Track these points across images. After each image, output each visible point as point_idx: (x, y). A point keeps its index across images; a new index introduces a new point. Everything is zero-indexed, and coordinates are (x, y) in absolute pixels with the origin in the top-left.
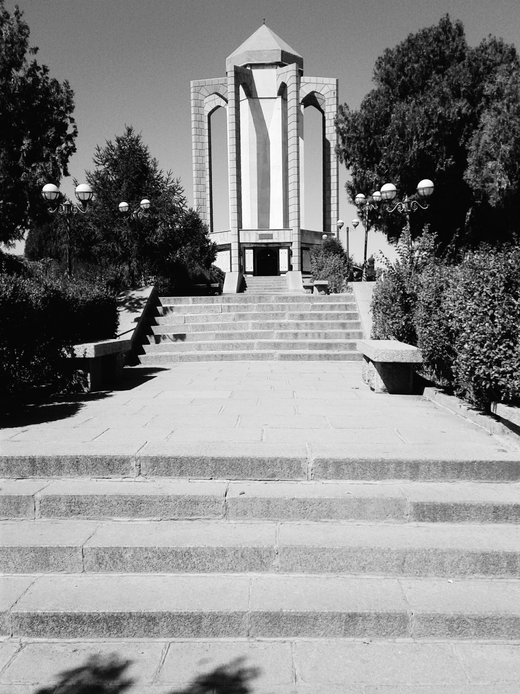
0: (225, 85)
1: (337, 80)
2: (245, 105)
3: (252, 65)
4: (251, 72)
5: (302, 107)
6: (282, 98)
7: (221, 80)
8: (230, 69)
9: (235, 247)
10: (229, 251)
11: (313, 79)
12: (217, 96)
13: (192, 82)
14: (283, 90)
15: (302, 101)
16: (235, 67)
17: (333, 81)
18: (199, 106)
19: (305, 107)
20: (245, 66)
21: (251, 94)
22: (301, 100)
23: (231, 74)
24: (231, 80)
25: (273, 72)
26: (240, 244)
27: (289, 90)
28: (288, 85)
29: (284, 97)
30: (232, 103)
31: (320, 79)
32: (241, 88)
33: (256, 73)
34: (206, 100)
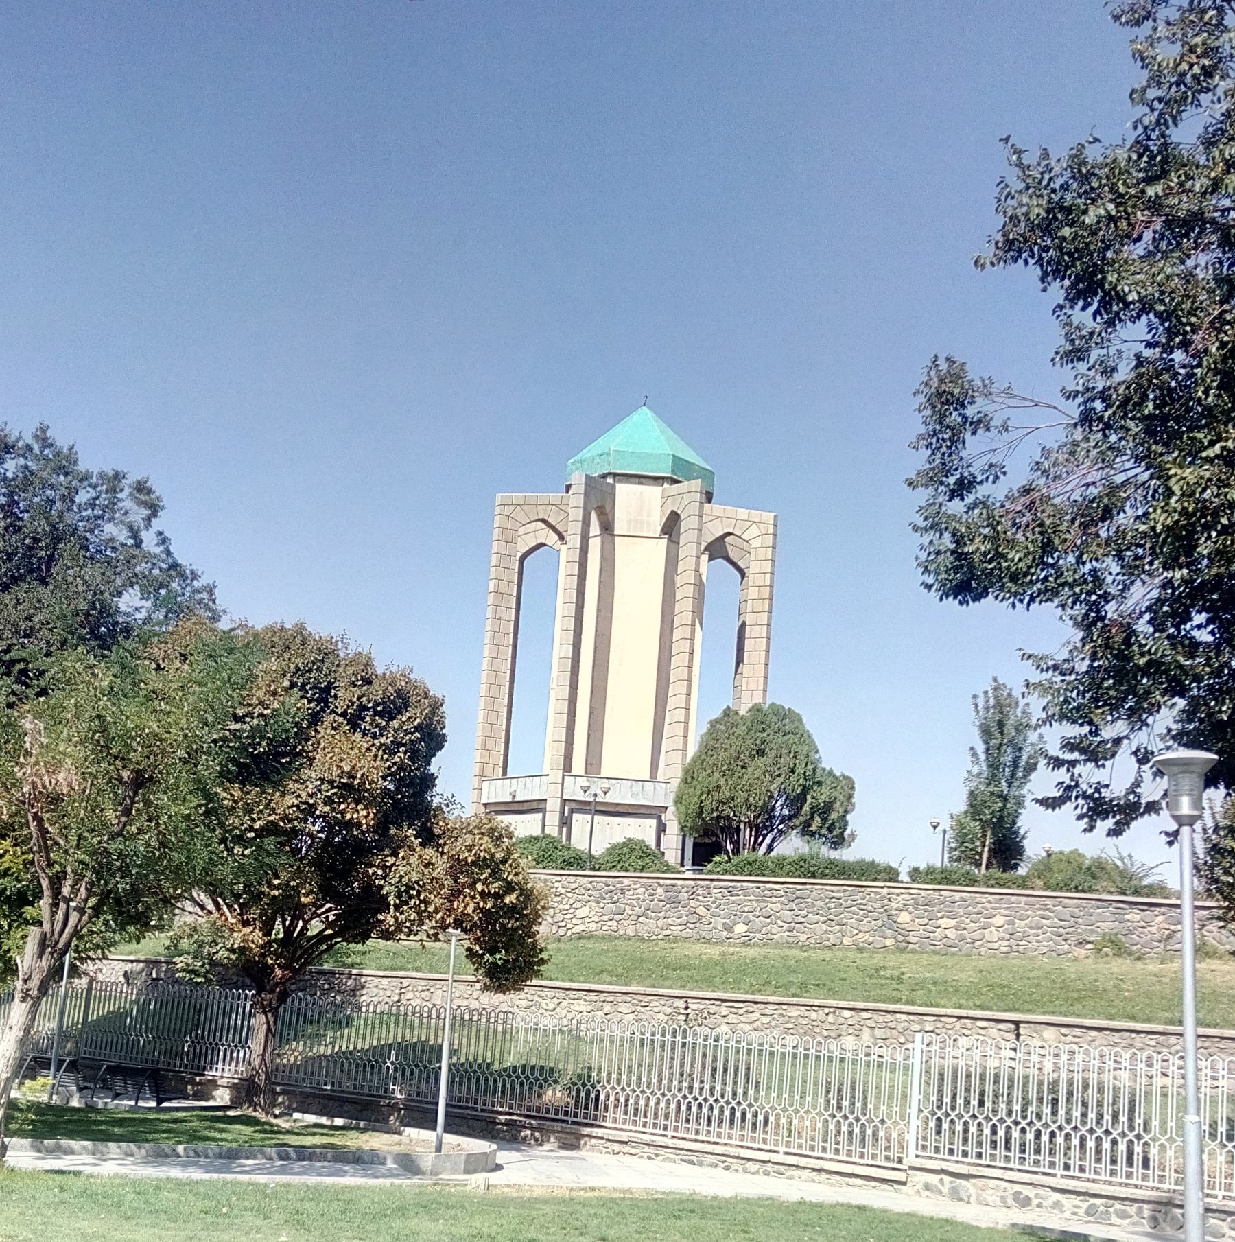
0: (560, 507)
1: (775, 516)
2: (595, 545)
3: (615, 475)
4: (613, 487)
5: (705, 558)
6: (670, 540)
7: (556, 497)
8: (577, 480)
9: (553, 806)
10: (540, 815)
11: (730, 510)
12: (542, 525)
13: (499, 496)
14: (671, 526)
15: (706, 549)
16: (587, 476)
17: (769, 517)
18: (509, 537)
19: (710, 560)
20: (605, 476)
21: (607, 528)
22: (704, 545)
23: (579, 489)
24: (576, 499)
25: (654, 492)
26: (564, 802)
27: (684, 526)
28: (682, 517)
29: (674, 538)
30: (574, 541)
31: (743, 513)
32: (594, 515)
33: (624, 492)
34: (521, 531)
